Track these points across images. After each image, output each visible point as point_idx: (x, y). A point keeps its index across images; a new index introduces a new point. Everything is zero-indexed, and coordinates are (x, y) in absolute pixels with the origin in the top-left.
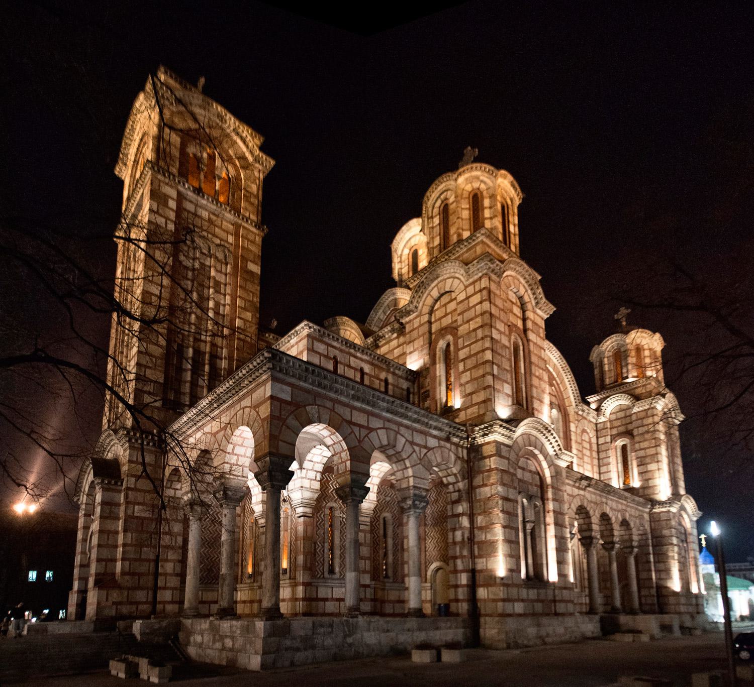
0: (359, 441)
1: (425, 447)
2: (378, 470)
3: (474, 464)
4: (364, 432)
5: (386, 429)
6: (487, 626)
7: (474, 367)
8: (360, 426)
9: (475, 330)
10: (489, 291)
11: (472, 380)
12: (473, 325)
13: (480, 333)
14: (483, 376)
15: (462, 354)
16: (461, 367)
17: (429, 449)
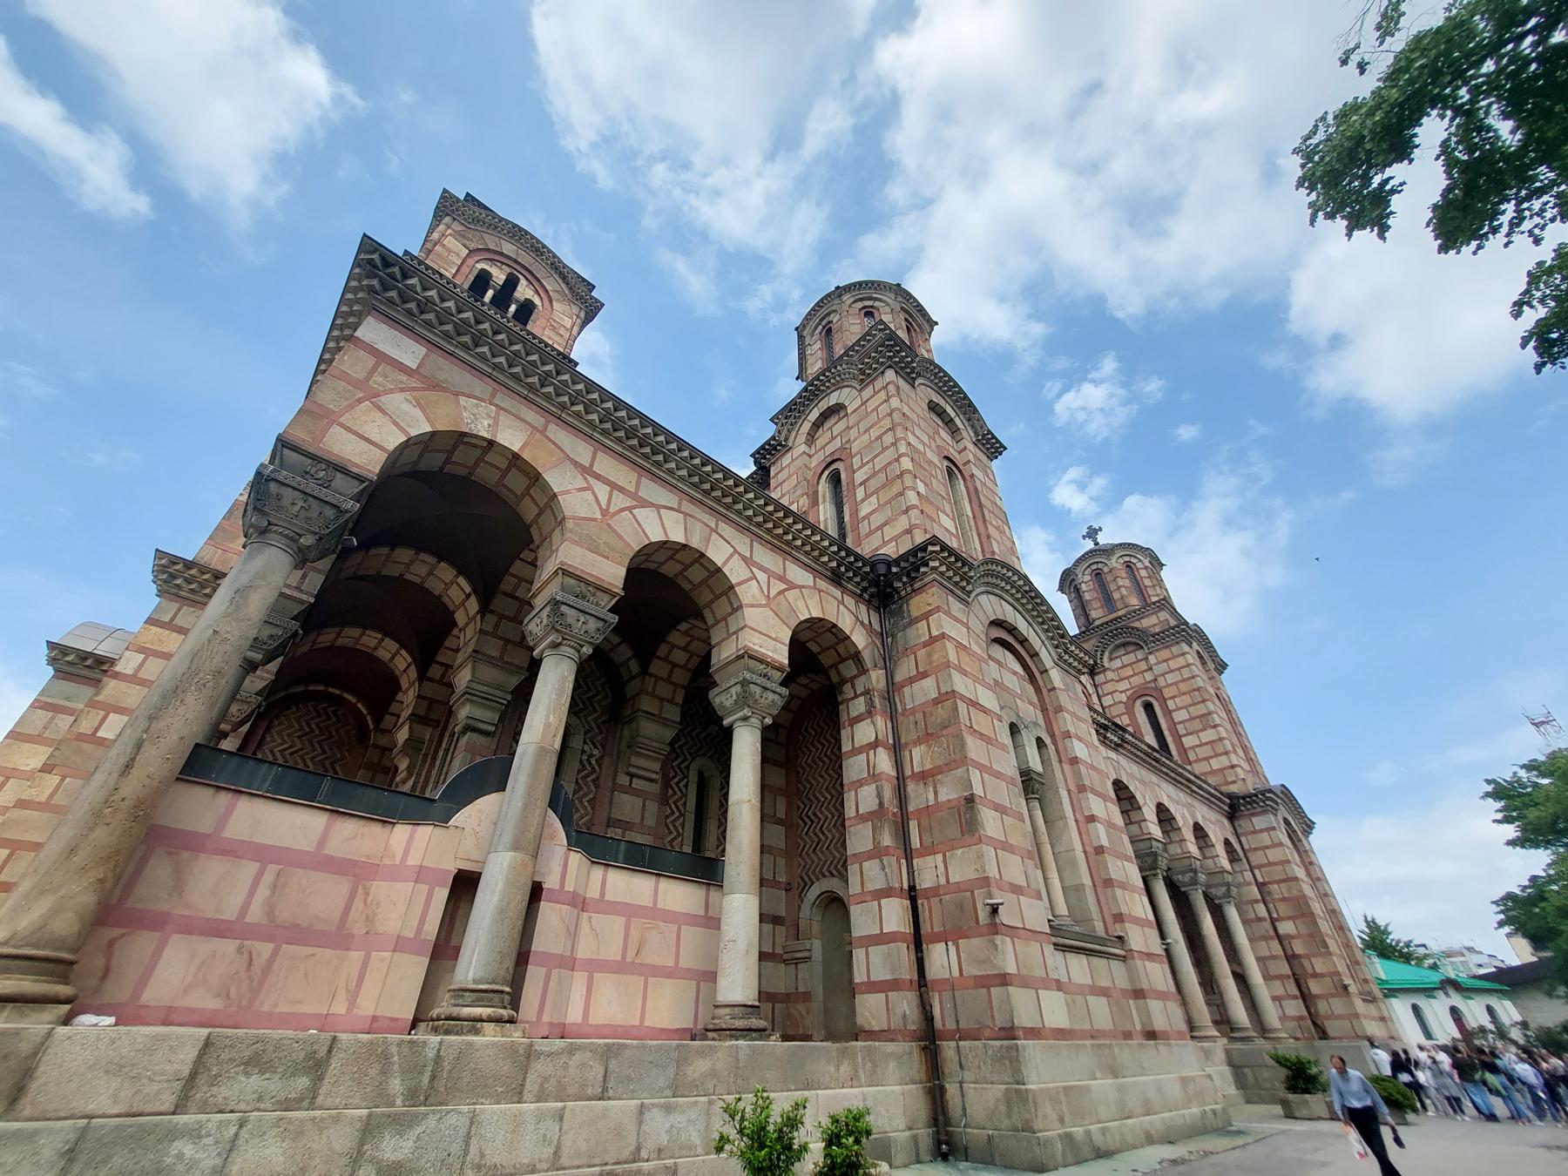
0: (605, 512)
1: (782, 579)
2: (685, 649)
3: (893, 636)
4: (620, 501)
5: (686, 514)
6: (968, 1076)
7: (883, 487)
8: (614, 486)
9: (879, 437)
10: (898, 388)
11: (880, 507)
12: (874, 433)
13: (888, 439)
14: (902, 494)
15: (859, 477)
16: (860, 494)
17: (792, 586)
